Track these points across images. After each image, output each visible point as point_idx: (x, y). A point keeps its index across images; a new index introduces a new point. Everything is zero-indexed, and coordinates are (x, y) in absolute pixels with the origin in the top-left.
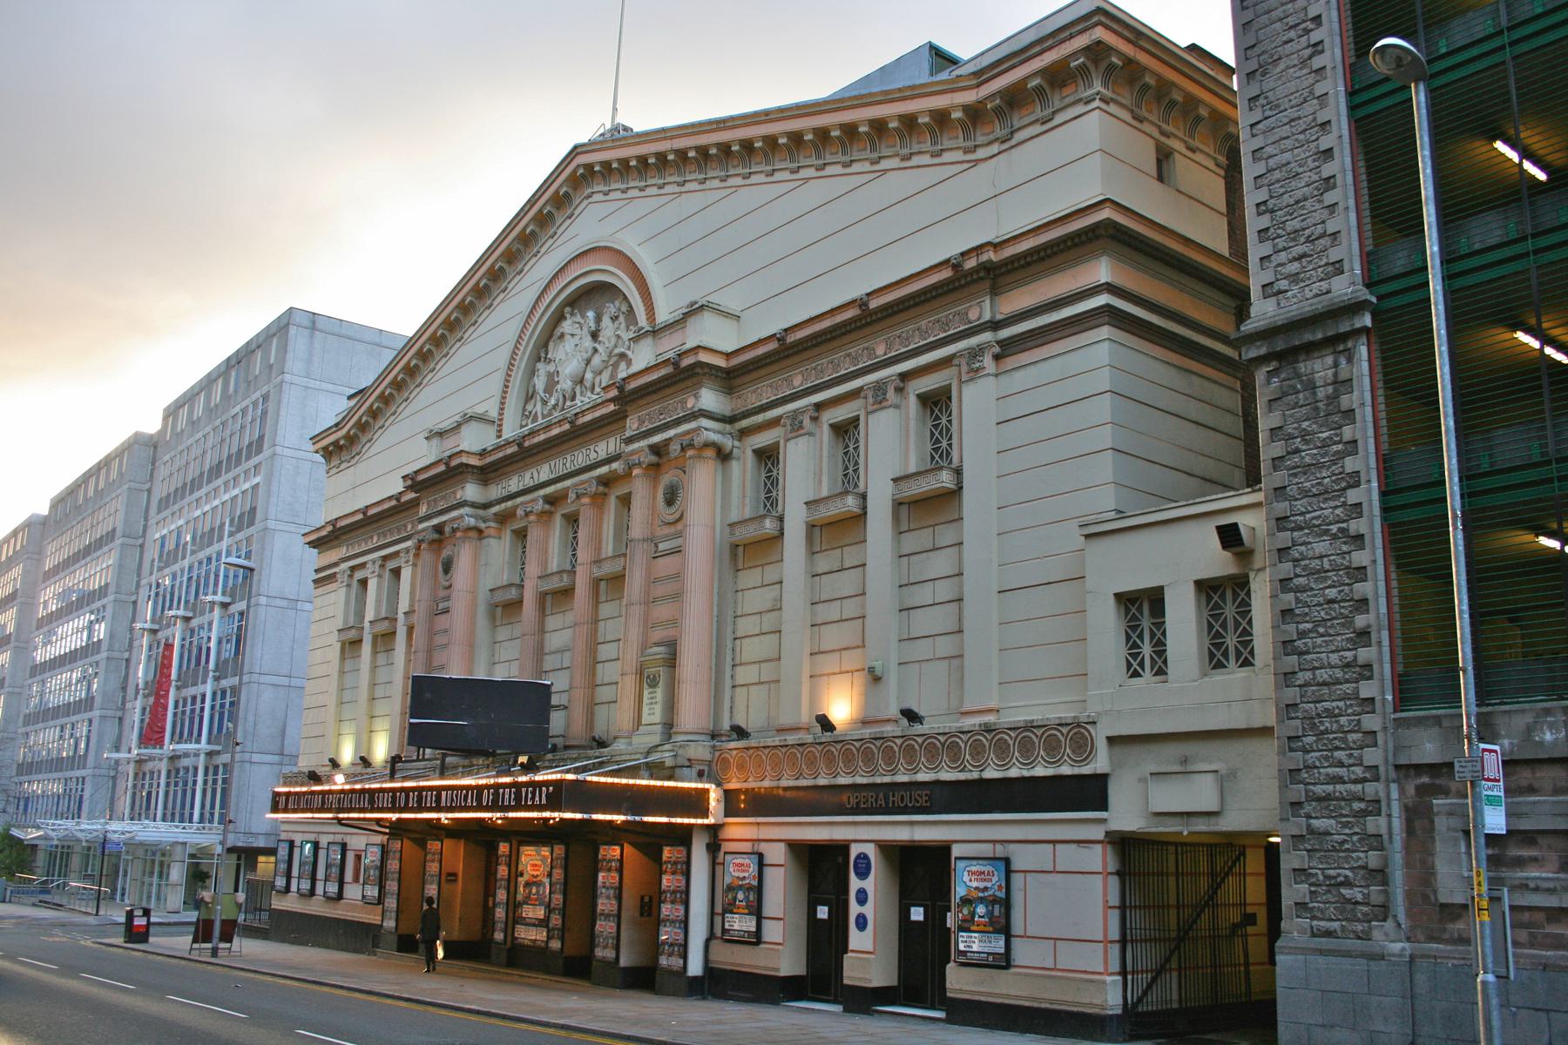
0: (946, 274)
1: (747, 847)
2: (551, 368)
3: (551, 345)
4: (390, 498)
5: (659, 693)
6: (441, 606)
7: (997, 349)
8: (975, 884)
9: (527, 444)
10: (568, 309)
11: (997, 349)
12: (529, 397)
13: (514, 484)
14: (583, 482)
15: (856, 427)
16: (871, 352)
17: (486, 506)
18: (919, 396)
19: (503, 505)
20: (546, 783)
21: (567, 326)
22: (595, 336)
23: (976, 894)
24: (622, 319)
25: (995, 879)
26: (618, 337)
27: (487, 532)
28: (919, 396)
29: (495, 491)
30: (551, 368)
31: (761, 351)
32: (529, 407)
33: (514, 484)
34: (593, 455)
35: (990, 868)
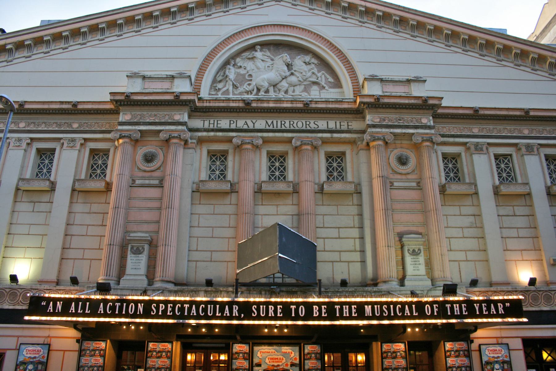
0: (70, 106)
1: (494, 341)
2: (242, 71)
3: (238, 60)
4: (69, 103)
5: (421, 259)
6: (138, 182)
7: (29, 141)
8: (492, 355)
9: (254, 105)
10: (259, 47)
11: (29, 141)
12: (214, 81)
13: (224, 123)
14: (308, 137)
15: (53, 154)
16: (471, 130)
17: (191, 130)
18: (37, 149)
19: (212, 134)
20: (503, 302)
21: (259, 54)
22: (289, 66)
23: (28, 360)
24: (313, 66)
25: (503, 352)
26: (313, 73)
27: (190, 145)
28: (37, 149)
29: (197, 123)
30: (242, 71)
31: (461, 112)
32: (220, 86)
33: (224, 123)
34: (313, 126)
35: (500, 348)
